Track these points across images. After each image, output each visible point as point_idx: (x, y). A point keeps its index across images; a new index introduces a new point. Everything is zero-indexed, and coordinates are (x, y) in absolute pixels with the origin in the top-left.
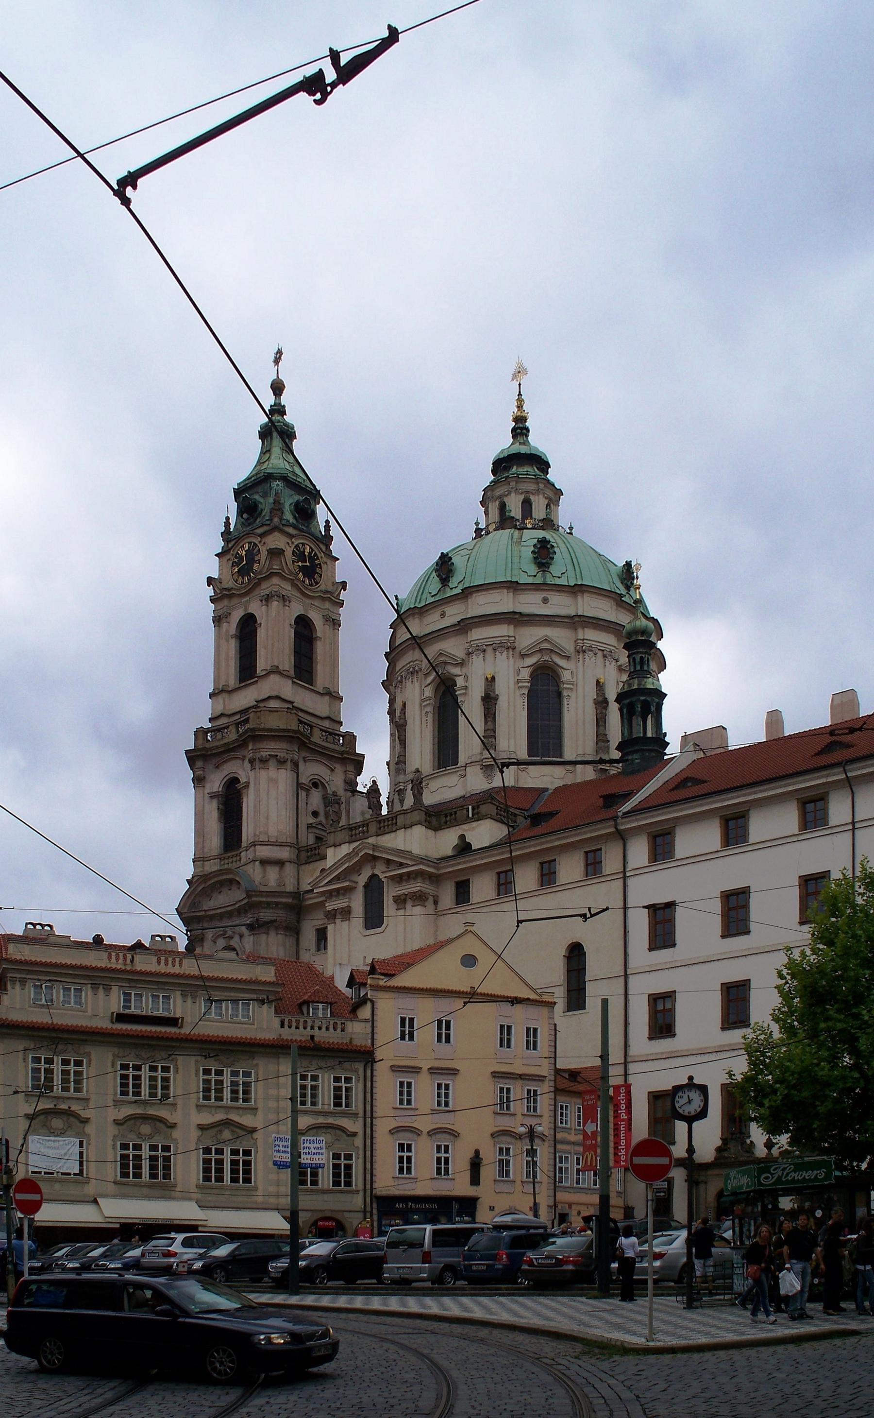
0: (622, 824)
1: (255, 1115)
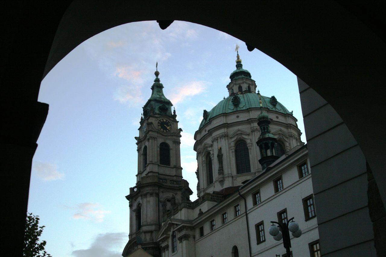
0: (241, 192)
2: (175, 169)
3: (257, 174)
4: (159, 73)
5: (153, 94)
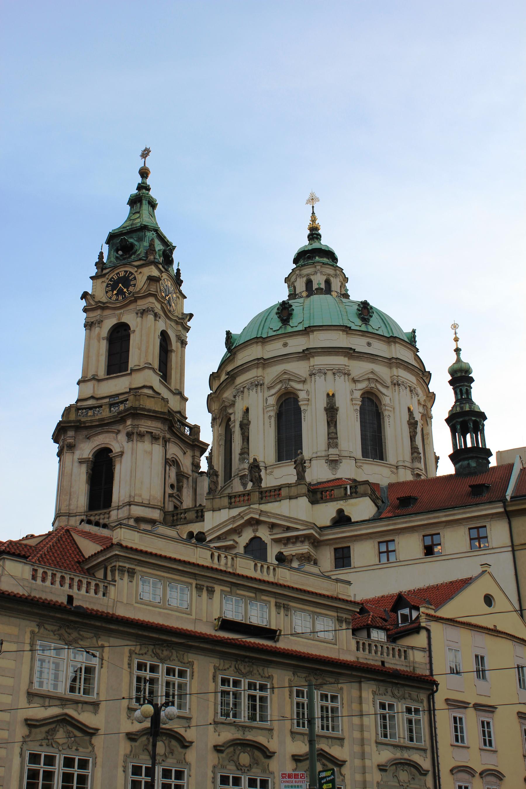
1: (342, 746)
2: (178, 397)
3: (401, 471)
4: (148, 170)
5: (132, 213)
